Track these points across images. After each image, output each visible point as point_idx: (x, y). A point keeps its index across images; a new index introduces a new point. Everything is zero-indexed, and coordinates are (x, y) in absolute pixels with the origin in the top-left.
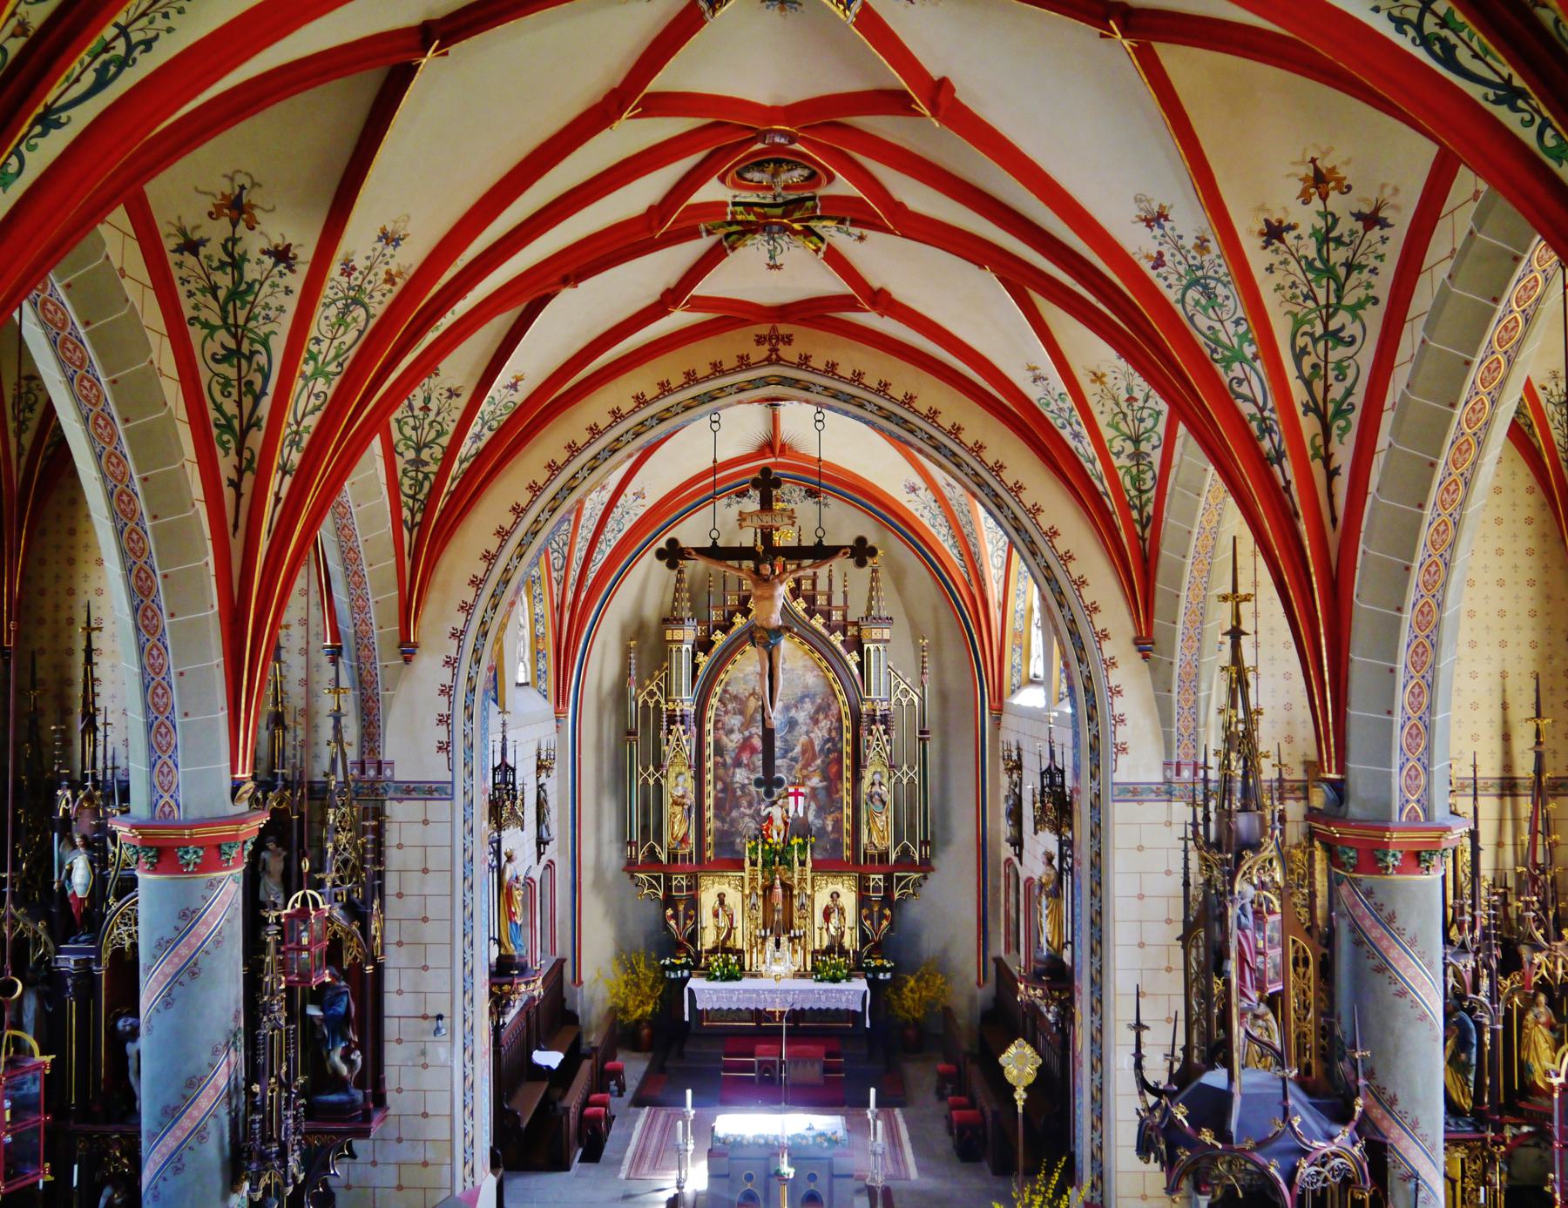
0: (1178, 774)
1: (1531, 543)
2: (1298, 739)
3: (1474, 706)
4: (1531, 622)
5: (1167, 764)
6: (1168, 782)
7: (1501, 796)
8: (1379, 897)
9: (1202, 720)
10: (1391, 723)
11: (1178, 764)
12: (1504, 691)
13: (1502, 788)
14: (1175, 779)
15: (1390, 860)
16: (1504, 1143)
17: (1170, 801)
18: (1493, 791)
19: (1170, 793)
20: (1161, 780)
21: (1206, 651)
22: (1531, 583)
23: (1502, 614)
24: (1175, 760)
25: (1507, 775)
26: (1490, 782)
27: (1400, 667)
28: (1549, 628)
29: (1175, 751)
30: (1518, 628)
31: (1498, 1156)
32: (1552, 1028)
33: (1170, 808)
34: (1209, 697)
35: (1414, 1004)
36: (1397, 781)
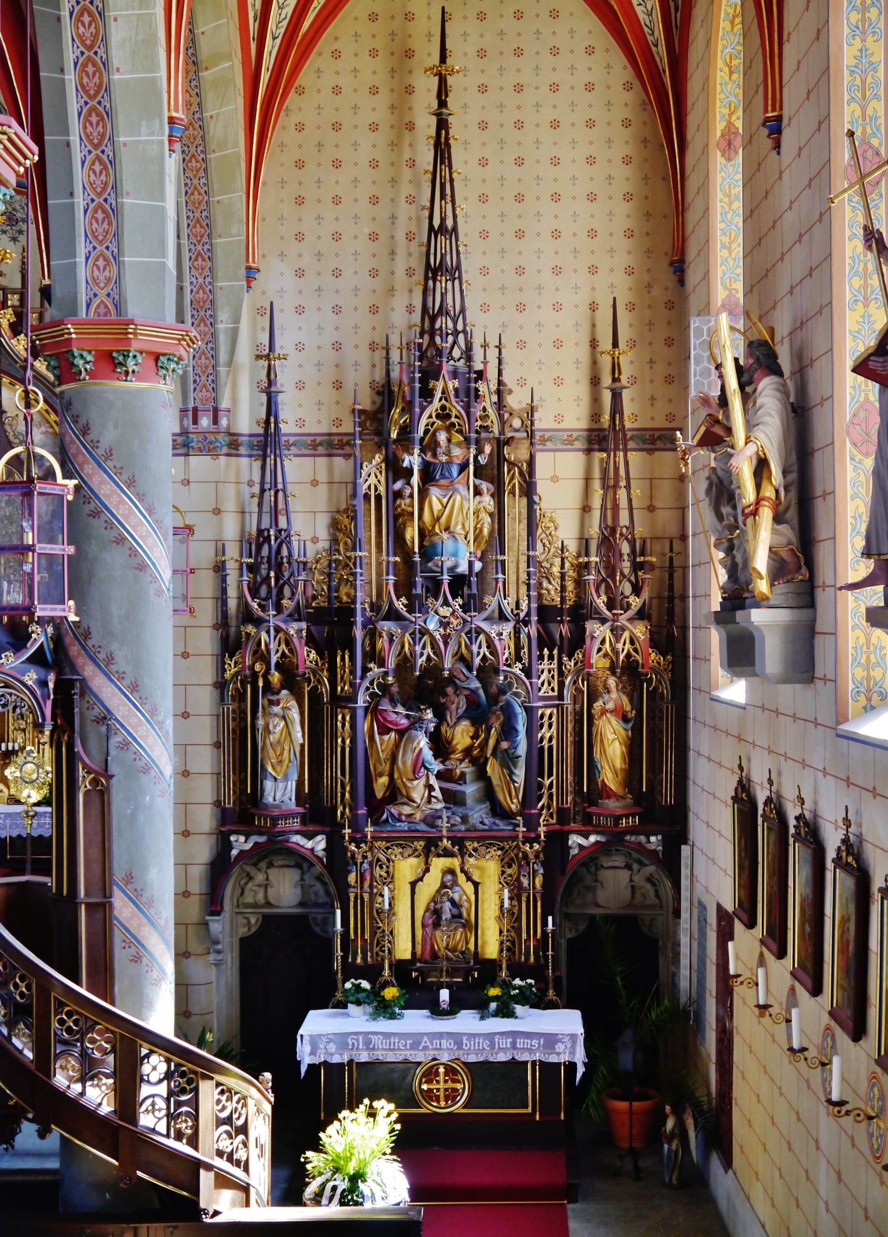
0: (195, 421)
1: (627, 150)
2: (349, 386)
3: (558, 344)
4: (627, 243)
5: (183, 411)
6: (184, 432)
7: (588, 451)
8: (76, 407)
9: (223, 357)
10: (72, 205)
11: (195, 410)
12: (594, 325)
13: (590, 441)
14: (192, 428)
15: (79, 362)
16: (537, 839)
17: (187, 455)
18: (578, 445)
19: (186, 445)
20: (178, 431)
21: (220, 273)
22: (628, 197)
23: (592, 234)
24: (191, 405)
25: (596, 426)
26: (575, 434)
27: (74, 139)
28: (649, 251)
29: (192, 395)
30: (612, 250)
31: (531, 856)
32: (625, 719)
33: (187, 463)
34: (234, 335)
35: (109, 526)
36: (82, 273)
